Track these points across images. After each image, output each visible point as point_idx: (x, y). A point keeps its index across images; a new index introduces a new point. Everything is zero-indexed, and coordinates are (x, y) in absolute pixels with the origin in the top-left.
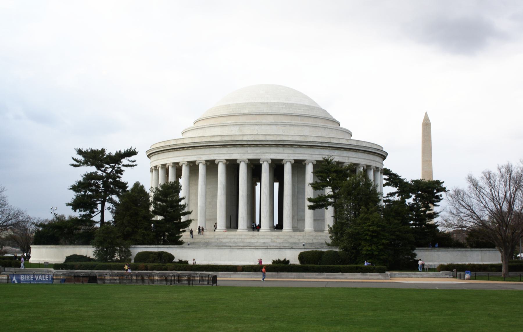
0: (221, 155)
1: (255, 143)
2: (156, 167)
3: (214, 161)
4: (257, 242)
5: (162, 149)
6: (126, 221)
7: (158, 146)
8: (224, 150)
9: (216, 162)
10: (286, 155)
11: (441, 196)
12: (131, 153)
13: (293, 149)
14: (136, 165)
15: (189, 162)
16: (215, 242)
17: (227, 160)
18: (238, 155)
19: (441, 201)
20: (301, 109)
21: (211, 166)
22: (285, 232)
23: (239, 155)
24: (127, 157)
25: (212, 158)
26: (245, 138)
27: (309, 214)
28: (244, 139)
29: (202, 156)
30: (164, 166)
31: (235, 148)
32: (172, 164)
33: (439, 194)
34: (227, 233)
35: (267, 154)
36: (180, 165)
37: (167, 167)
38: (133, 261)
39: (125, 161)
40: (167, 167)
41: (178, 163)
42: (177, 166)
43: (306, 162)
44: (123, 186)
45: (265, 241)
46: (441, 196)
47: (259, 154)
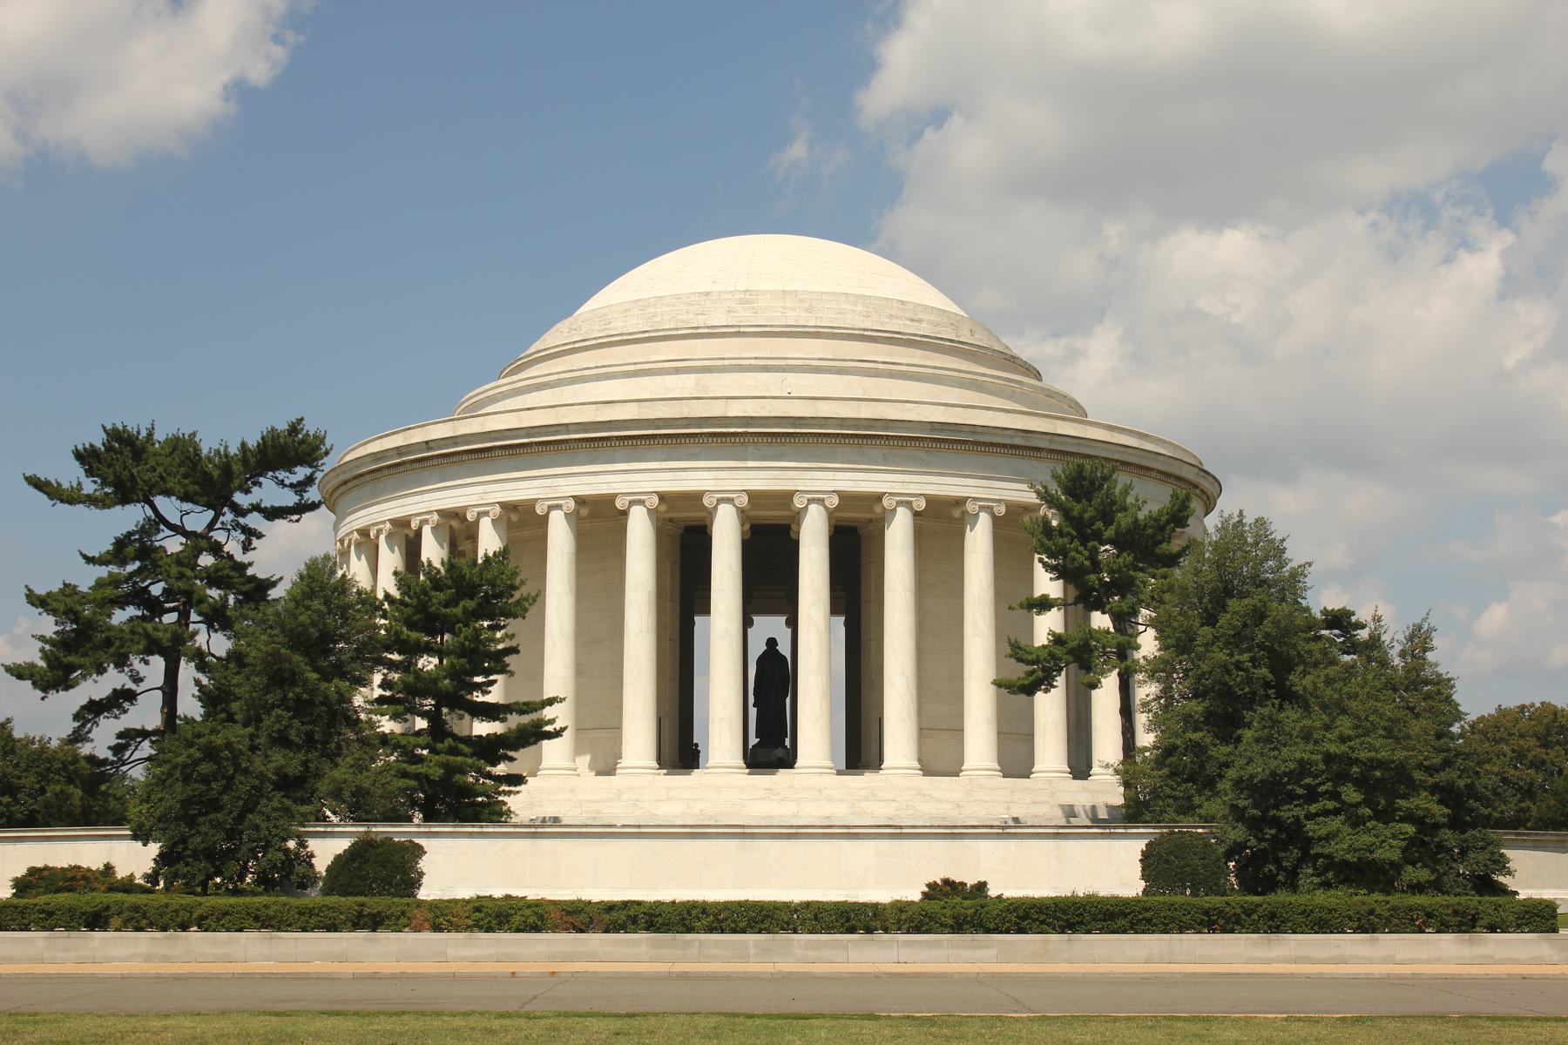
3: (610, 499)
15: (508, 507)
17: (663, 497)
20: (920, 321)
21: (599, 523)
25: (604, 490)
36: (470, 517)
37: (414, 525)
41: (456, 515)
42: (455, 524)
44: (258, 590)
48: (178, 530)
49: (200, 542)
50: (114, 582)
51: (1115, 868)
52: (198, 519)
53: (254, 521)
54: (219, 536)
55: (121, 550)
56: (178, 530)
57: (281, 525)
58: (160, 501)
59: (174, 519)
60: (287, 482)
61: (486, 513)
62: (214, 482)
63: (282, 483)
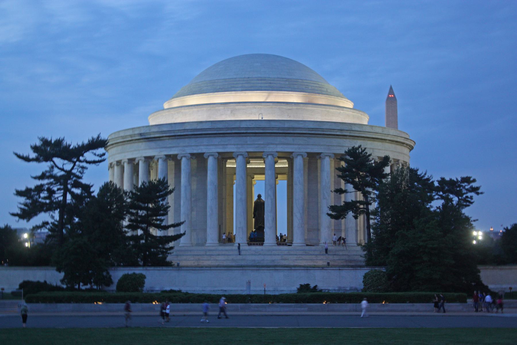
0: (212, 147)
1: (257, 131)
2: (119, 163)
4: (263, 260)
5: (130, 139)
6: (102, 232)
7: (122, 134)
8: (217, 140)
9: (205, 156)
10: (296, 146)
11: (471, 198)
12: (97, 144)
13: (305, 139)
14: (104, 160)
16: (201, 258)
17: (219, 153)
18: (233, 146)
19: (471, 205)
22: (318, 246)
23: (236, 146)
24: (92, 149)
25: (200, 151)
26: (243, 125)
27: (326, 223)
28: (242, 126)
29: (186, 148)
30: (131, 161)
31: (231, 138)
32: (143, 159)
33: (469, 195)
34: (221, 248)
35: (272, 146)
37: (136, 161)
38: (114, 287)
39: (89, 156)
40: (136, 161)
43: (322, 155)
45: (274, 258)
46: (471, 198)
47: (262, 146)
48: (62, 170)
49: (69, 174)
50: (42, 185)
51: (353, 280)
52: (68, 166)
53: (84, 164)
54: (74, 171)
55: (43, 177)
56: (62, 170)
57: (93, 166)
58: (56, 160)
59: (60, 166)
60: (97, 154)
61: (161, 158)
62: (73, 154)
63: (95, 154)
